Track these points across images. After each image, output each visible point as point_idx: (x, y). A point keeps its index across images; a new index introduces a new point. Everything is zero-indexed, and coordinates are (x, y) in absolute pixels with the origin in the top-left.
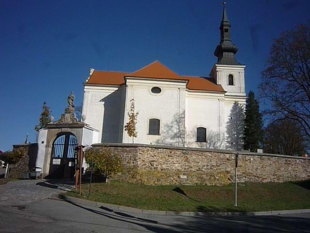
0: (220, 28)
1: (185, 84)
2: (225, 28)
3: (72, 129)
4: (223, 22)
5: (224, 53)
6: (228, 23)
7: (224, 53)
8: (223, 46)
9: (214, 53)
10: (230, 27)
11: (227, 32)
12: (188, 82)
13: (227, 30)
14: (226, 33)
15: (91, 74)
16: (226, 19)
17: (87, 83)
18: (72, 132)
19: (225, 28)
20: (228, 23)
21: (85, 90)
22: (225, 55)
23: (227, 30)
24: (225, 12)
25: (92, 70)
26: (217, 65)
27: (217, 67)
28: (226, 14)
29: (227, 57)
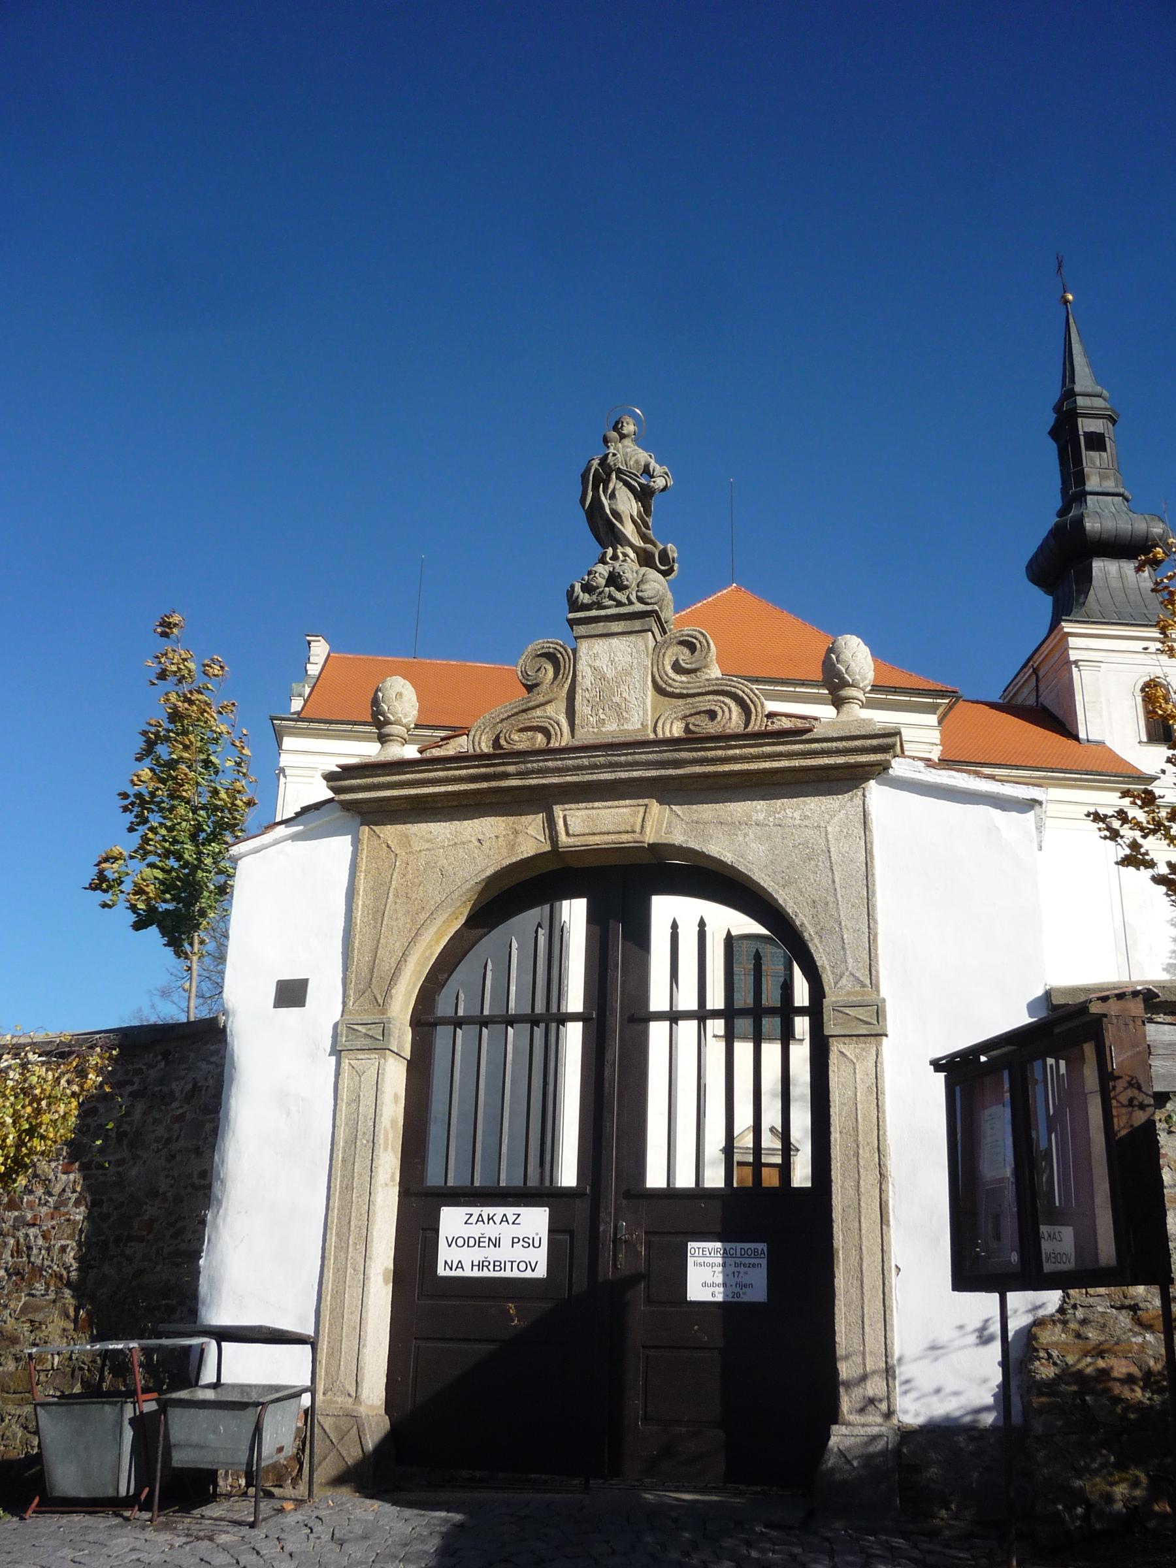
0: (1055, 433)
1: (933, 719)
2: (1086, 426)
3: (706, 811)
4: (1069, 394)
5: (1098, 565)
6: (1098, 402)
7: (1098, 565)
8: (1092, 525)
9: (1029, 568)
10: (1114, 422)
11: (1103, 448)
12: (950, 707)
13: (1097, 442)
14: (1095, 455)
15: (313, 670)
16: (1084, 380)
17: (299, 717)
18: (720, 849)
19: (1086, 426)
20: (1098, 402)
21: (285, 760)
22: (1106, 574)
23: (1097, 442)
24: (1077, 348)
25: (320, 650)
26: (1068, 627)
27: (1072, 641)
28: (1086, 352)
29: (1115, 584)
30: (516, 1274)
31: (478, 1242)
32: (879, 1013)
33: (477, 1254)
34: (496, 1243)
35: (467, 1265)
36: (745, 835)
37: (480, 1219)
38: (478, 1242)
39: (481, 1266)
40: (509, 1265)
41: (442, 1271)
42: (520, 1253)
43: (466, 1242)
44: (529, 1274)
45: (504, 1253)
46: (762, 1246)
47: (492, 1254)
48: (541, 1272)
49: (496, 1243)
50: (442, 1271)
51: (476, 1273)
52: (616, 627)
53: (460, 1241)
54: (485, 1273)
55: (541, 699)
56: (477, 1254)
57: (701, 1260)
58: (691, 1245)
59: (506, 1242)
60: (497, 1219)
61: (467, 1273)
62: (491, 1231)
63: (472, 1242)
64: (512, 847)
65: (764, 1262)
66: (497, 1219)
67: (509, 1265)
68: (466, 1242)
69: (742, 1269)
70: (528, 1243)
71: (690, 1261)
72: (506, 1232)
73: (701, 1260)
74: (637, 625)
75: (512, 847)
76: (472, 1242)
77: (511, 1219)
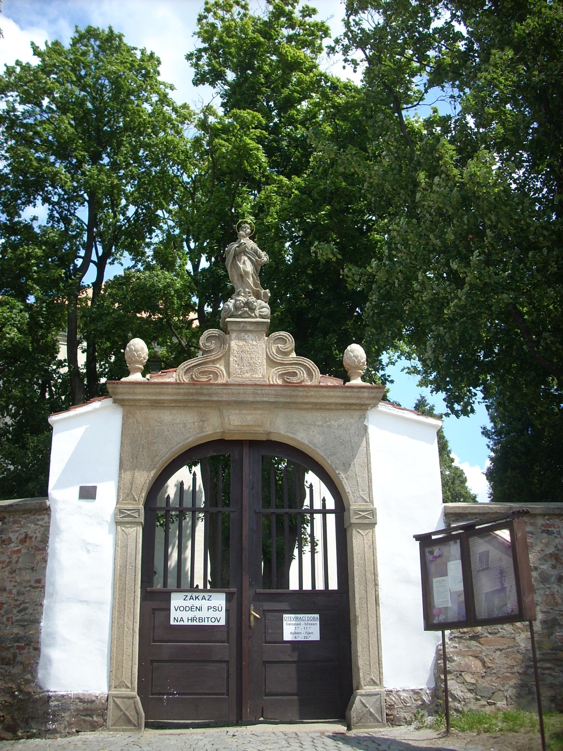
30: (210, 623)
31: (191, 609)
32: (373, 513)
33: (190, 614)
34: (200, 609)
35: (185, 620)
36: (313, 431)
37: (191, 598)
38: (191, 609)
39: (192, 620)
40: (206, 619)
41: (172, 622)
42: (211, 614)
43: (185, 609)
44: (216, 623)
45: (204, 614)
46: (317, 616)
47: (198, 614)
48: (223, 622)
49: (200, 609)
50: (172, 622)
51: (190, 623)
52: (249, 328)
53: (182, 608)
54: (195, 623)
55: (212, 358)
56: (190, 614)
57: (289, 622)
58: (285, 616)
59: (205, 609)
60: (200, 598)
61: (186, 623)
62: (197, 603)
63: (187, 609)
64: (202, 428)
65: (318, 623)
66: (200, 598)
67: (206, 619)
68: (185, 609)
69: (308, 626)
70: (215, 609)
71: (285, 623)
72: (205, 604)
73: (289, 622)
74: (260, 328)
75: (202, 428)
76: (187, 609)
77: (207, 598)
